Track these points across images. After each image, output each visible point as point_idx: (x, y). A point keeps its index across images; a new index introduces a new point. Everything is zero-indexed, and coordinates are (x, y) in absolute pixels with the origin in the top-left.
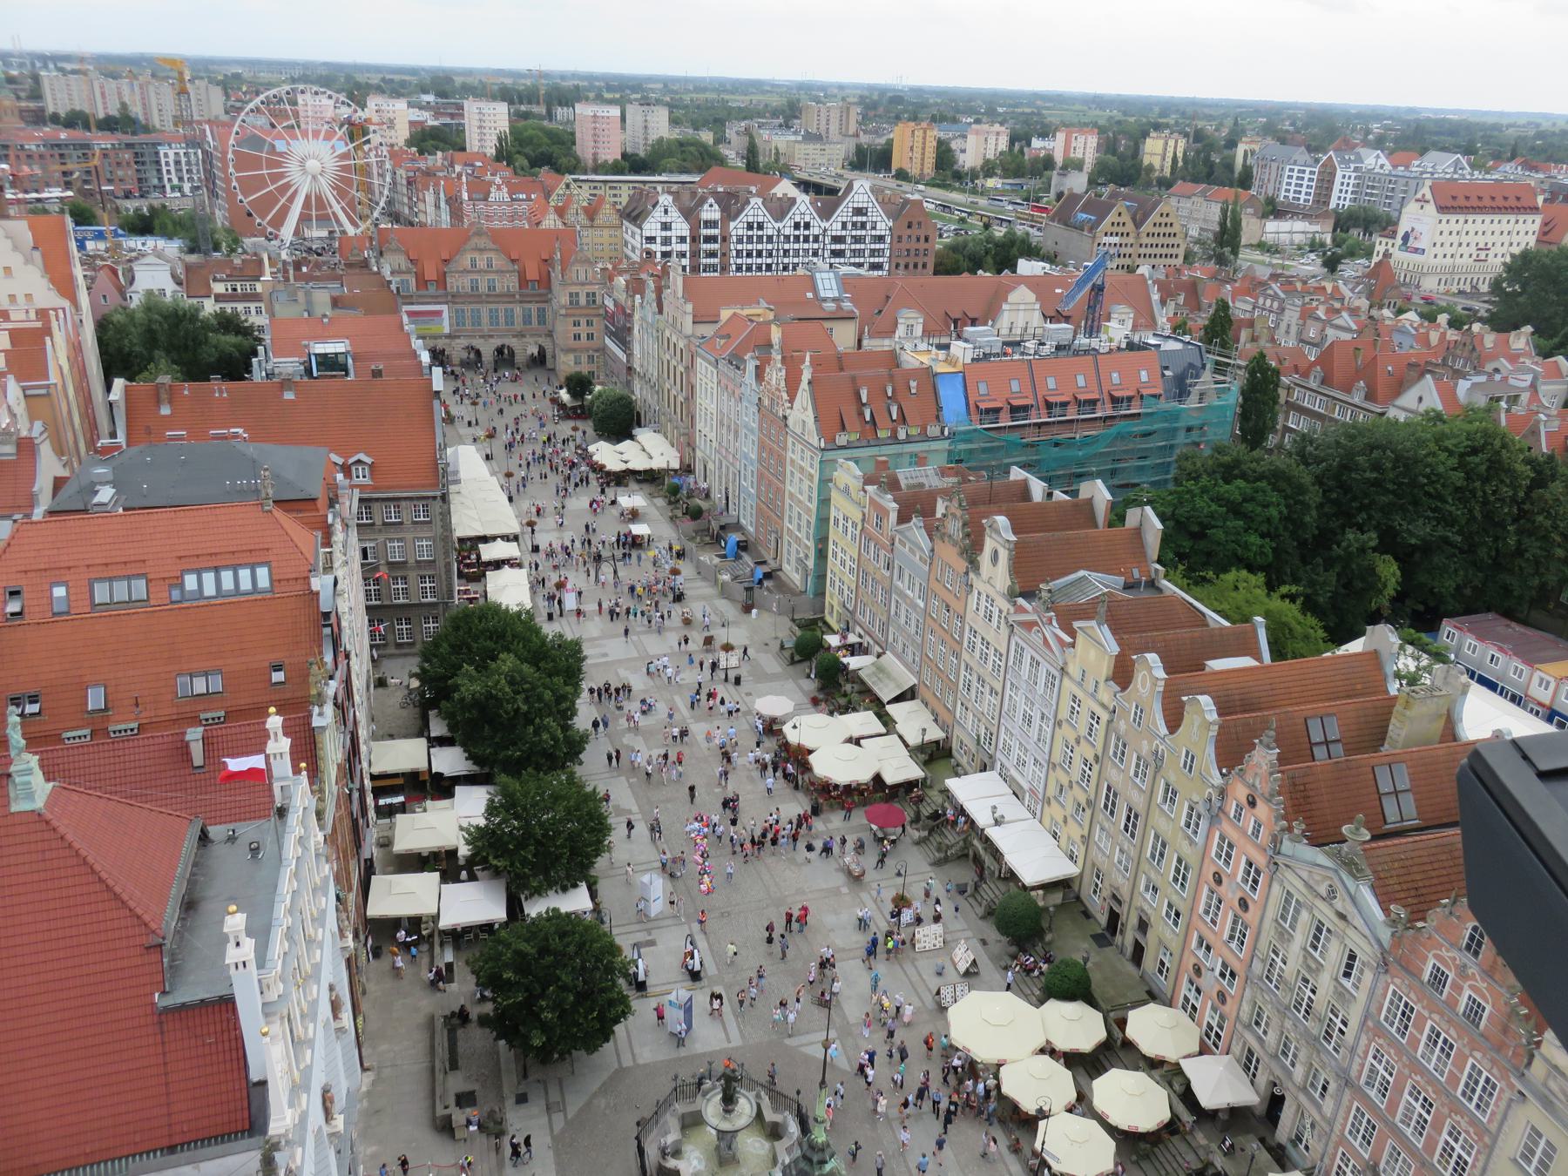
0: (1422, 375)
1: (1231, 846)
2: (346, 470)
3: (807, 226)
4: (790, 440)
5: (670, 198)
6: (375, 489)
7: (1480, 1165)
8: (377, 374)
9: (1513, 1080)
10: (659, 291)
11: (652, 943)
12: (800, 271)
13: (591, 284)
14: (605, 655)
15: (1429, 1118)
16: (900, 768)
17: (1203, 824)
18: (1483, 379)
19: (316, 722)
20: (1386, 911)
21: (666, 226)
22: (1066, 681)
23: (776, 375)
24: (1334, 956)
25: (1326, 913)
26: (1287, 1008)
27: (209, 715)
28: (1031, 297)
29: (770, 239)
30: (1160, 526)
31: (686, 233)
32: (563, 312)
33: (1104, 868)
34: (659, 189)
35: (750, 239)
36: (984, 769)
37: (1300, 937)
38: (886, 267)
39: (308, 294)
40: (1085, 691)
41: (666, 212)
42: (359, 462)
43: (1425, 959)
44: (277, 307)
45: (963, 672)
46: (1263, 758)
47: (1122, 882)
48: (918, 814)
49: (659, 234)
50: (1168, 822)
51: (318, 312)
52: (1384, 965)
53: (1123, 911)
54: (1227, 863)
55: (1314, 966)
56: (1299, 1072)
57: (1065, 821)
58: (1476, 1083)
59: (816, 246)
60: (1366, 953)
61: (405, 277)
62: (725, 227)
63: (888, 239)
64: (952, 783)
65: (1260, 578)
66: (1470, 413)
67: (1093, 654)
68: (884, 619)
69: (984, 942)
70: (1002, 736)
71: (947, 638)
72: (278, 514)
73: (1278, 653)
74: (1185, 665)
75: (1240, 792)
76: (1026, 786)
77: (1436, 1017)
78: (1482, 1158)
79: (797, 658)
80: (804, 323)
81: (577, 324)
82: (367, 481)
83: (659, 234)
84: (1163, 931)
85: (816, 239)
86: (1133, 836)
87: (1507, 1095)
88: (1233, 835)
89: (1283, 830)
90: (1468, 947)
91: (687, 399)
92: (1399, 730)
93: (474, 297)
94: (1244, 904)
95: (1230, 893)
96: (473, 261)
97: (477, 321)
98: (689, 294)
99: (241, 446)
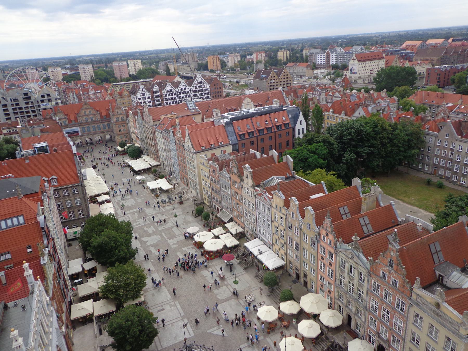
0: (359, 107)
1: (324, 248)
2: (49, 182)
3: (185, 89)
4: (186, 151)
5: (143, 86)
6: (59, 186)
7: (405, 326)
8: (55, 151)
9: (408, 301)
10: (142, 114)
11: (163, 309)
12: (183, 102)
13: (122, 114)
14: (140, 224)
15: (389, 316)
16: (231, 242)
17: (316, 243)
18: (375, 105)
19: (42, 262)
20: (367, 259)
21: (143, 94)
22: (273, 209)
23: (178, 134)
24: (356, 274)
25: (352, 263)
26: (347, 292)
27: (8, 266)
28: (250, 100)
30: (292, 160)
31: (150, 96)
32: (115, 124)
34: (140, 84)
35: (169, 95)
36: (255, 238)
37: (347, 271)
38: (210, 97)
39: (32, 129)
40: (278, 211)
41: (143, 90)
42: (53, 178)
43: (380, 271)
44: (23, 135)
45: (244, 211)
46: (327, 221)
47: (297, 263)
48: (238, 255)
49: (142, 97)
50: (306, 245)
51: (36, 134)
52: (370, 275)
53: (299, 272)
54: (324, 253)
55: (352, 278)
56: (353, 310)
58: (399, 303)
60: (364, 272)
61: (64, 120)
62: (161, 92)
64: (246, 244)
65: (324, 170)
66: (373, 115)
67: (278, 200)
68: (220, 199)
70: (258, 228)
71: (238, 202)
72: (24, 199)
74: (304, 199)
75: (324, 233)
76: (267, 241)
77: (385, 286)
78: (405, 324)
79: (197, 215)
80: (185, 118)
82: (56, 184)
83: (142, 97)
84: (311, 276)
86: (298, 250)
87: (408, 305)
89: (336, 241)
90: (390, 265)
91: (155, 144)
92: (364, 207)
93: (87, 123)
94: (330, 264)
95: (326, 262)
96: (85, 112)
97: (89, 130)
98: (150, 114)
99: (11, 180)
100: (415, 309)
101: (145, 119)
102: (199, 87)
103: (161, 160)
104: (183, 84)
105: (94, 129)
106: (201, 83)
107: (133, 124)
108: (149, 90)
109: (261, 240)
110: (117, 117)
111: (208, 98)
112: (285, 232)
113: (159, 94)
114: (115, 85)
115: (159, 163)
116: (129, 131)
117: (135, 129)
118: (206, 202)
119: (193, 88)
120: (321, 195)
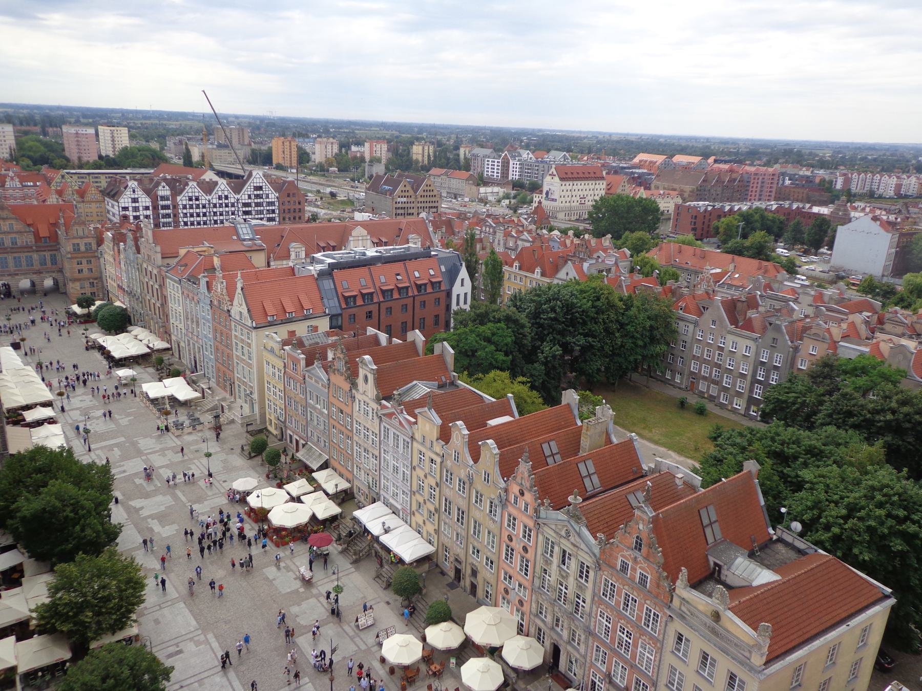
0: (566, 262)
1: (514, 519)
3: (226, 197)
4: (233, 324)
5: (136, 183)
7: (658, 659)
9: (666, 610)
10: (136, 240)
11: (180, 652)
12: (227, 224)
13: (87, 237)
14: (124, 471)
16: (325, 509)
17: (499, 510)
18: (594, 261)
20: (595, 538)
21: (135, 200)
22: (415, 444)
23: (220, 287)
24: (573, 566)
25: (566, 545)
26: (555, 600)
28: (365, 232)
30: (452, 351)
31: (149, 204)
32: (69, 256)
33: (449, 545)
34: (128, 177)
35: (191, 207)
36: (374, 501)
37: (556, 560)
38: (277, 219)
40: (426, 447)
41: (134, 191)
43: (617, 558)
45: (355, 448)
46: (524, 468)
47: (458, 550)
48: (339, 535)
50: (479, 513)
52: (599, 567)
53: (462, 567)
54: (514, 529)
56: (565, 634)
57: (424, 523)
58: (650, 616)
59: (233, 209)
60: (588, 561)
63: (277, 204)
64: (358, 513)
65: (506, 374)
66: (591, 278)
67: (428, 427)
68: (304, 423)
69: (388, 603)
70: (382, 481)
71: (343, 429)
73: (521, 413)
74: (477, 425)
75: (515, 489)
76: (399, 507)
77: (626, 587)
78: (658, 655)
79: (253, 454)
80: (233, 255)
81: (79, 263)
83: (131, 205)
84: (486, 573)
86: (462, 524)
87: (664, 619)
88: (514, 512)
89: (539, 505)
90: (636, 548)
91: (162, 305)
92: (585, 442)
94: (525, 549)
95: (517, 545)
98: (156, 240)
100: (678, 625)
101: (142, 251)
102: (257, 196)
103: (173, 338)
104: (223, 187)
106: (260, 188)
107: (111, 260)
108: (148, 192)
109: (387, 504)
110: (76, 241)
112: (437, 489)
113: (169, 202)
114: (68, 173)
115: (168, 346)
116: (101, 273)
117: (118, 272)
118: (272, 429)
119: (244, 198)
120: (506, 419)
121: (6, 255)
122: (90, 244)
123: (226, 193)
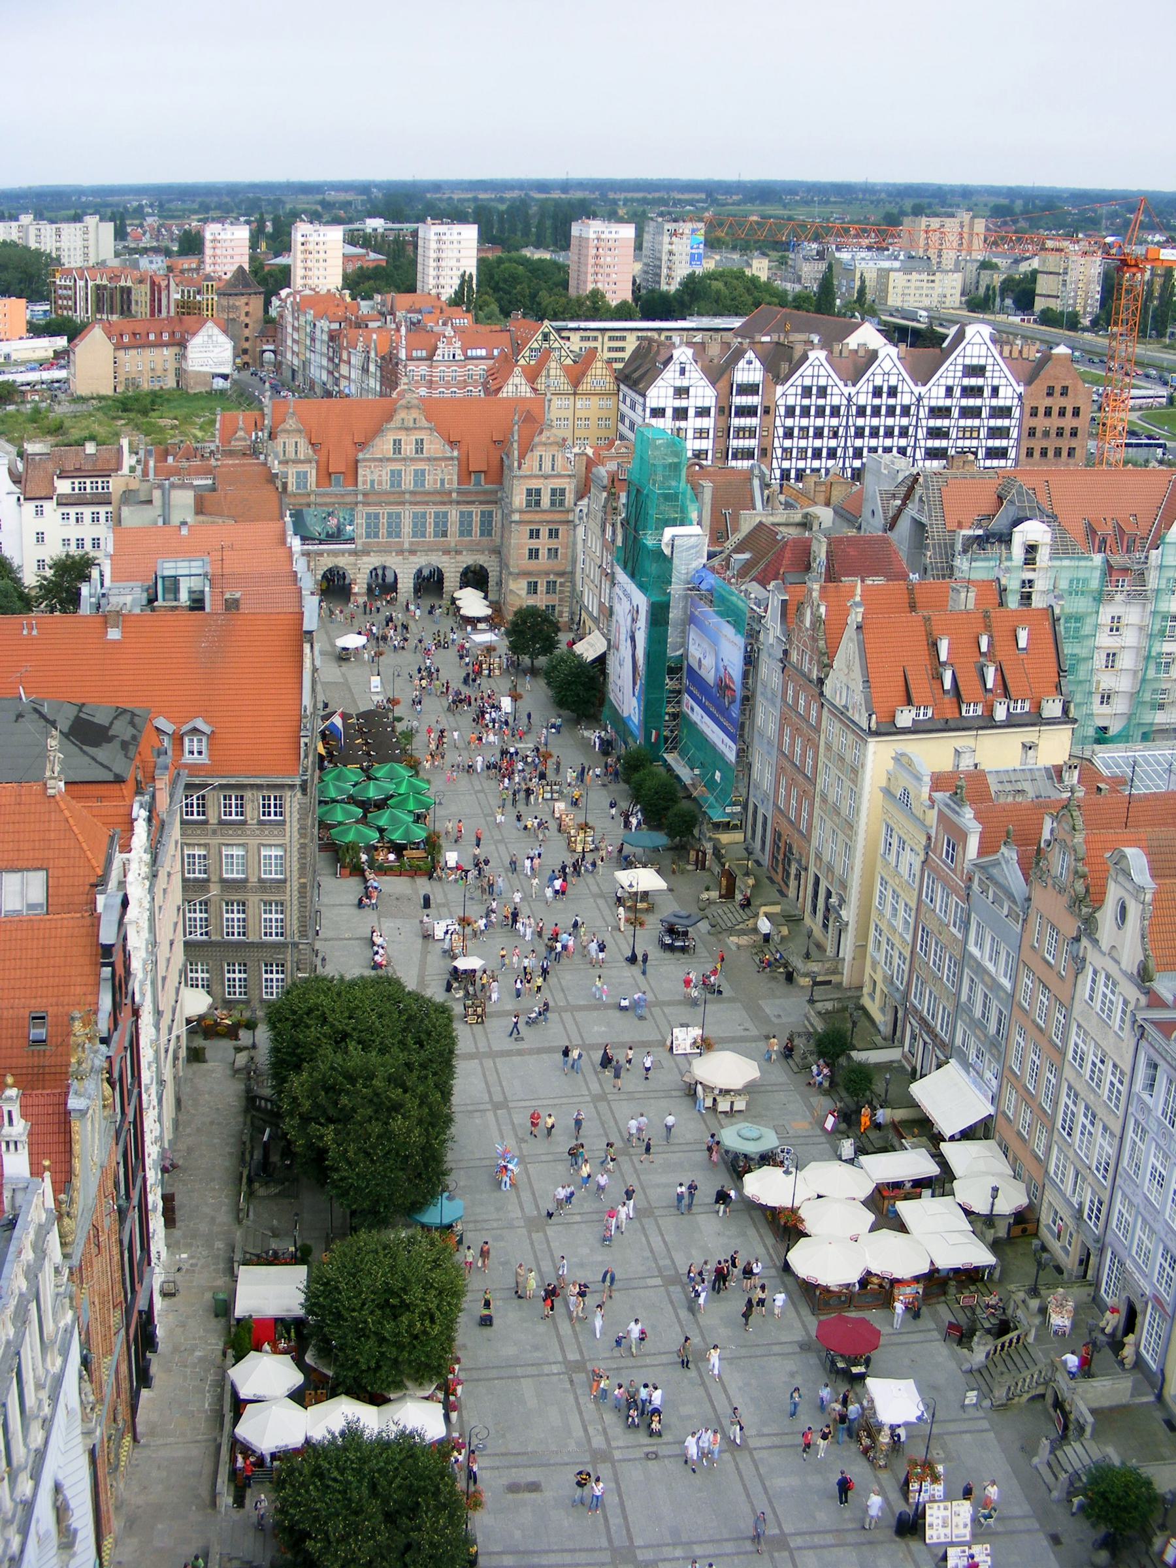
3: (893, 392)
5: (689, 352)
13: (560, 476)
29: (835, 411)
34: (676, 339)
35: (805, 412)
38: (1012, 454)
41: (683, 372)
45: (1064, 1099)
59: (905, 421)
63: (1016, 413)
69: (1055, 1539)
70: (1118, 1206)
81: (534, 534)
85: (906, 411)
96: (397, 443)
97: (394, 529)
102: (968, 392)
104: (887, 365)
105: (419, 528)
106: (977, 371)
111: (1001, 453)
114: (559, 330)
119: (935, 394)
121: (398, 509)
122: (563, 492)
123: (893, 381)
